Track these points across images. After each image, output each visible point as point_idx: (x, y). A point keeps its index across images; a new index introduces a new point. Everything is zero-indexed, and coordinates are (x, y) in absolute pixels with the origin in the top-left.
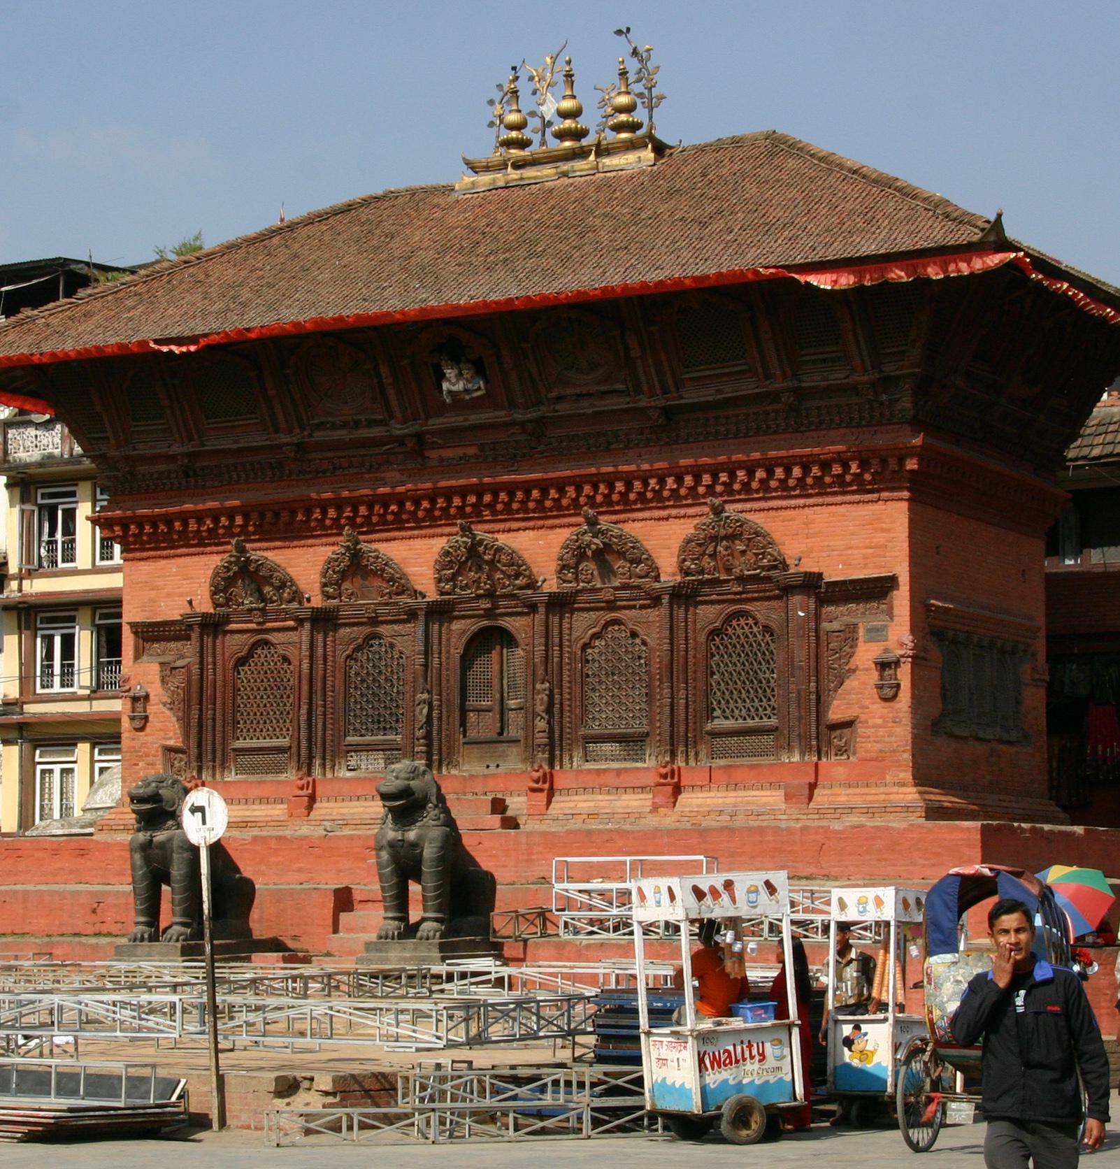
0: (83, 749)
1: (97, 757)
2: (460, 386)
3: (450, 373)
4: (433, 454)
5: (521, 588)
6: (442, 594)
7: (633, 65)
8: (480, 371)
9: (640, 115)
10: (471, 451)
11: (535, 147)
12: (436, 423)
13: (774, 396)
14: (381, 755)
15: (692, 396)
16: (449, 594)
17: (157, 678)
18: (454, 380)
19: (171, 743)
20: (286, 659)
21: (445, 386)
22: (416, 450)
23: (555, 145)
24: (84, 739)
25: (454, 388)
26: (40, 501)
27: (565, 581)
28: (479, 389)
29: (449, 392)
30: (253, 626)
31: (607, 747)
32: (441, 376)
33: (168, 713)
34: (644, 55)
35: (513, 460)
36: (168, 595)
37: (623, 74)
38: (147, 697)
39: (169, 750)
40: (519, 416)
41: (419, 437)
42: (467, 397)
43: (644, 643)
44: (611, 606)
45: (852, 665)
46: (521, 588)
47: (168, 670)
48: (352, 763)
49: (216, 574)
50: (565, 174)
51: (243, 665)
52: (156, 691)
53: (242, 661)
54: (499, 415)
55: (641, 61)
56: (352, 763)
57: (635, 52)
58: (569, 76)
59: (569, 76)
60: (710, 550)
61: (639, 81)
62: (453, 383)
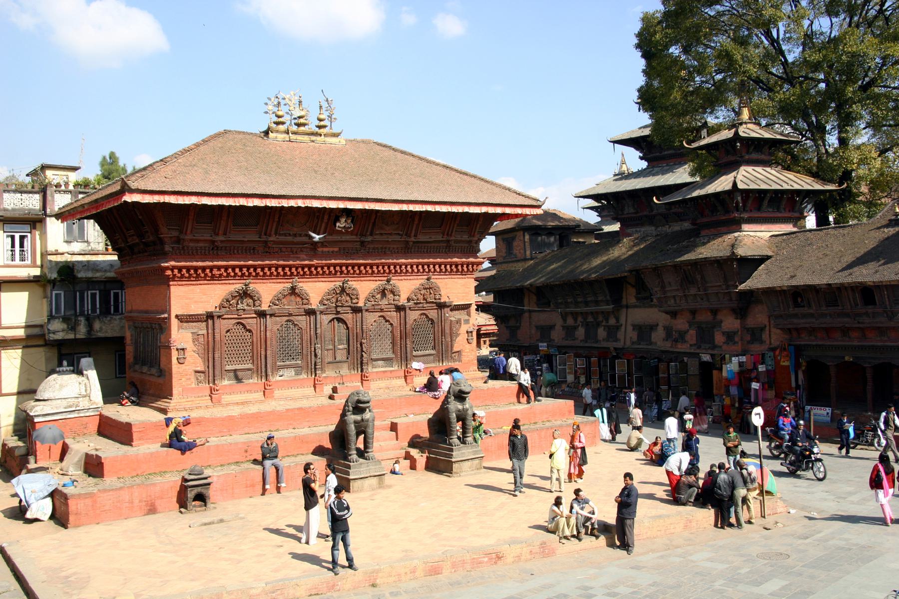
3: (343, 220)
4: (320, 250)
7: (325, 105)
10: (336, 249)
14: (293, 370)
15: (422, 238)
17: (191, 340)
19: (199, 369)
20: (250, 331)
21: (338, 224)
31: (380, 363)
35: (348, 255)
36: (196, 302)
39: (197, 372)
43: (391, 324)
44: (382, 310)
47: (196, 337)
48: (281, 373)
50: (313, 141)
52: (189, 345)
56: (281, 373)
60: (422, 292)
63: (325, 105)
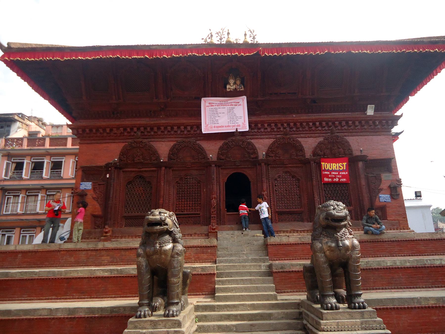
0: (17, 231)
1: (22, 232)
2: (233, 87)
3: (232, 81)
5: (253, 159)
6: (221, 159)
7: (248, 33)
8: (242, 83)
16: (223, 160)
18: (232, 84)
19: (97, 213)
24: (18, 227)
25: (231, 88)
26: (12, 161)
27: (270, 156)
28: (242, 88)
29: (229, 89)
30: (137, 170)
33: (96, 203)
34: (252, 31)
37: (245, 35)
38: (86, 195)
39: (94, 216)
42: (238, 90)
43: (298, 180)
45: (381, 187)
46: (253, 159)
49: (125, 147)
51: (129, 184)
53: (129, 183)
55: (251, 32)
58: (228, 34)
59: (228, 34)
61: (250, 37)
63: (248, 33)
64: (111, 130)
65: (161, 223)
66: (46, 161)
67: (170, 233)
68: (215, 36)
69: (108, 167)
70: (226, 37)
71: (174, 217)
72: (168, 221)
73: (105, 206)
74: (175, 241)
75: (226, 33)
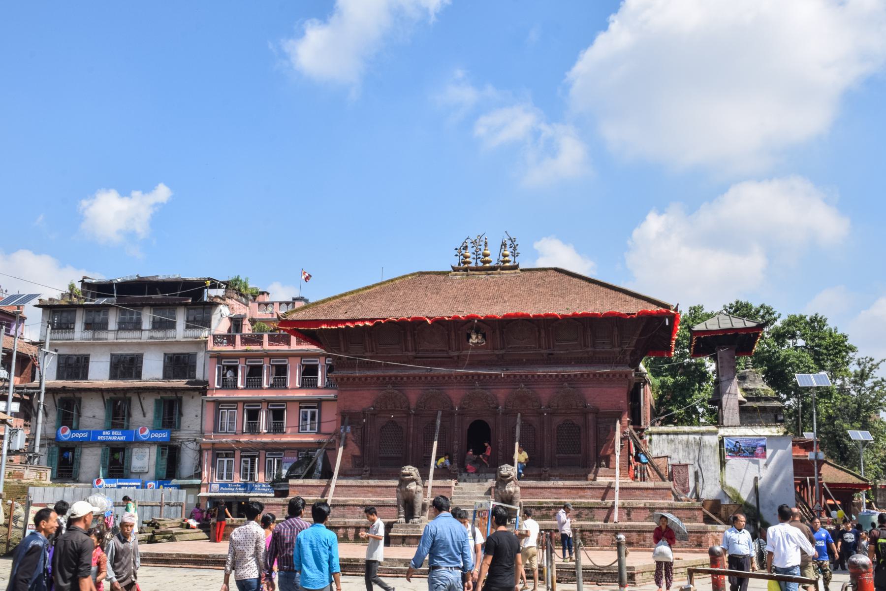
3: (474, 337)
7: (508, 243)
8: (484, 336)
9: (510, 258)
11: (473, 265)
12: (464, 352)
13: (588, 352)
22: (456, 362)
23: (480, 264)
32: (469, 337)
39: (354, 457)
40: (497, 352)
41: (458, 357)
54: (489, 352)
57: (510, 239)
62: (474, 340)
63: (508, 243)
64: (366, 379)
65: (409, 475)
66: (266, 364)
67: (413, 480)
68: (470, 245)
69: (364, 414)
70: (483, 247)
71: (417, 471)
72: (414, 473)
73: (363, 448)
74: (417, 484)
75: (483, 243)
